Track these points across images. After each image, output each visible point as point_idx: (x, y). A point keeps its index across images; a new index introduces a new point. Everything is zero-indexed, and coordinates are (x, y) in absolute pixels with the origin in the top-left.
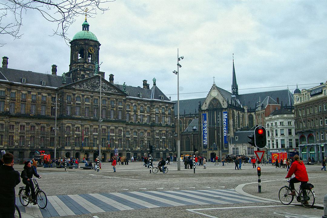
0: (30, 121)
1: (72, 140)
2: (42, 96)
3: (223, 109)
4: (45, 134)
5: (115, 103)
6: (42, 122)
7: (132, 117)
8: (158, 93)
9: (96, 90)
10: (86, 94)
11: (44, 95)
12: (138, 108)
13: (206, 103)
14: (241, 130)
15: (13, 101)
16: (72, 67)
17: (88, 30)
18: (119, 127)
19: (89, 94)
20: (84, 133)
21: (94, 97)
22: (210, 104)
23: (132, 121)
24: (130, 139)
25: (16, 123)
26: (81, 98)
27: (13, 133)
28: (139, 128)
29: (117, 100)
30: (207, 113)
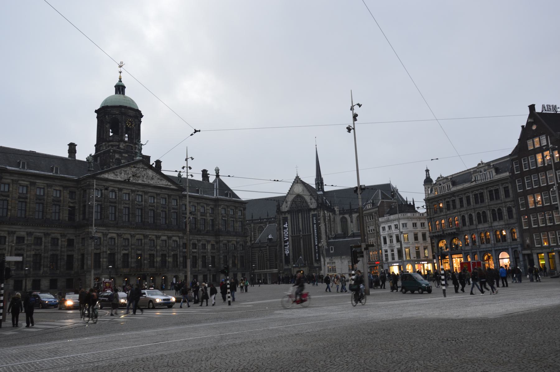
0: (33, 230)
3: (311, 210)
6: (53, 231)
8: (223, 188)
9: (140, 182)
13: (286, 203)
14: (336, 237)
15: (4, 198)
16: (100, 147)
17: (123, 94)
18: (173, 236)
19: (129, 188)
22: (292, 203)
25: (10, 233)
27: (3, 249)
28: (199, 239)
30: (289, 216)
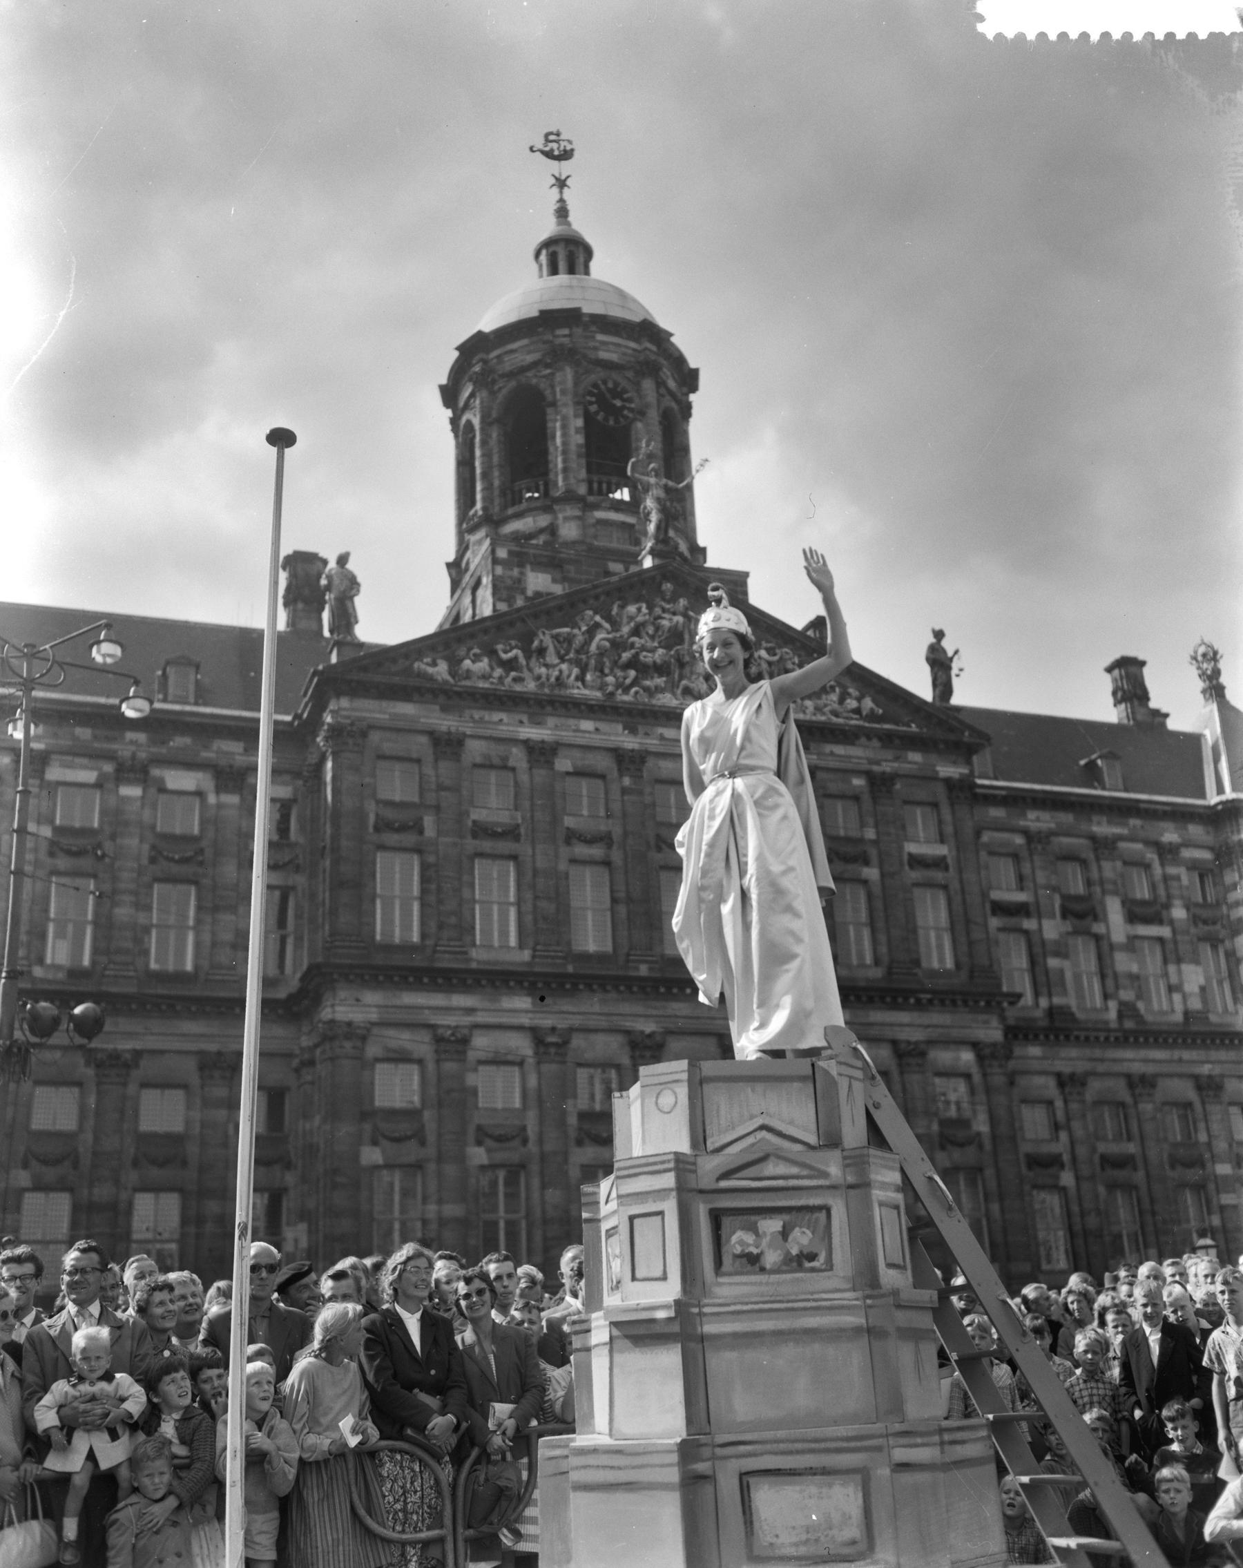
1: (440, 1202)
2: (162, 790)
4: (184, 1163)
5: (871, 821)
7: (1053, 962)
10: (566, 736)
11: (180, 780)
12: (1102, 882)
19: (597, 740)
20: (573, 1120)
21: (651, 762)
23: (1057, 1000)
24: (1067, 1179)
26: (524, 778)
28: (1137, 1068)
29: (880, 784)
